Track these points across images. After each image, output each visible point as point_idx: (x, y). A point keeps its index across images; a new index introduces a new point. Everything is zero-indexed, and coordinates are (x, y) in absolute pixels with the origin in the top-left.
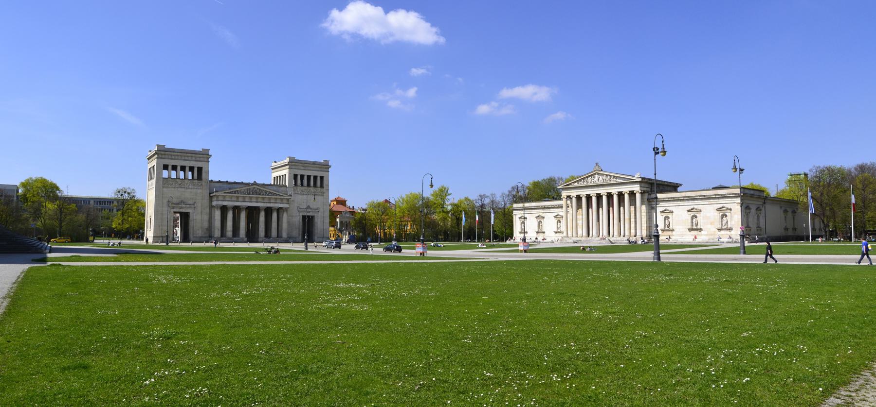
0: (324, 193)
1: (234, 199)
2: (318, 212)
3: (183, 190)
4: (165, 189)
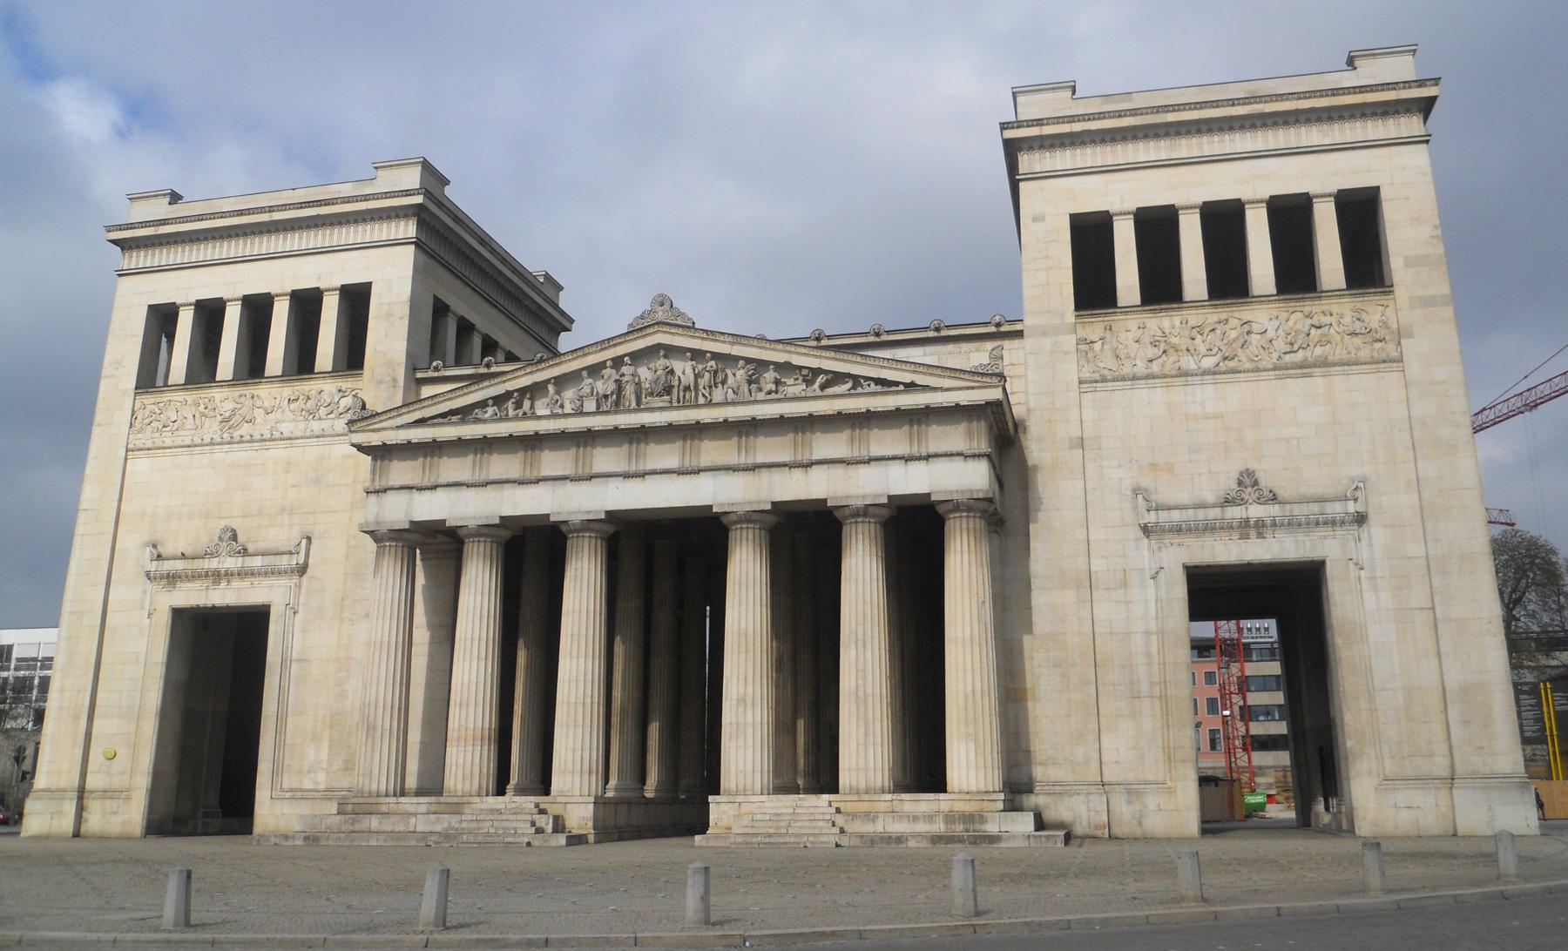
0: (1399, 335)
1: (504, 465)
2: (1361, 519)
3: (240, 454)
4: (138, 465)
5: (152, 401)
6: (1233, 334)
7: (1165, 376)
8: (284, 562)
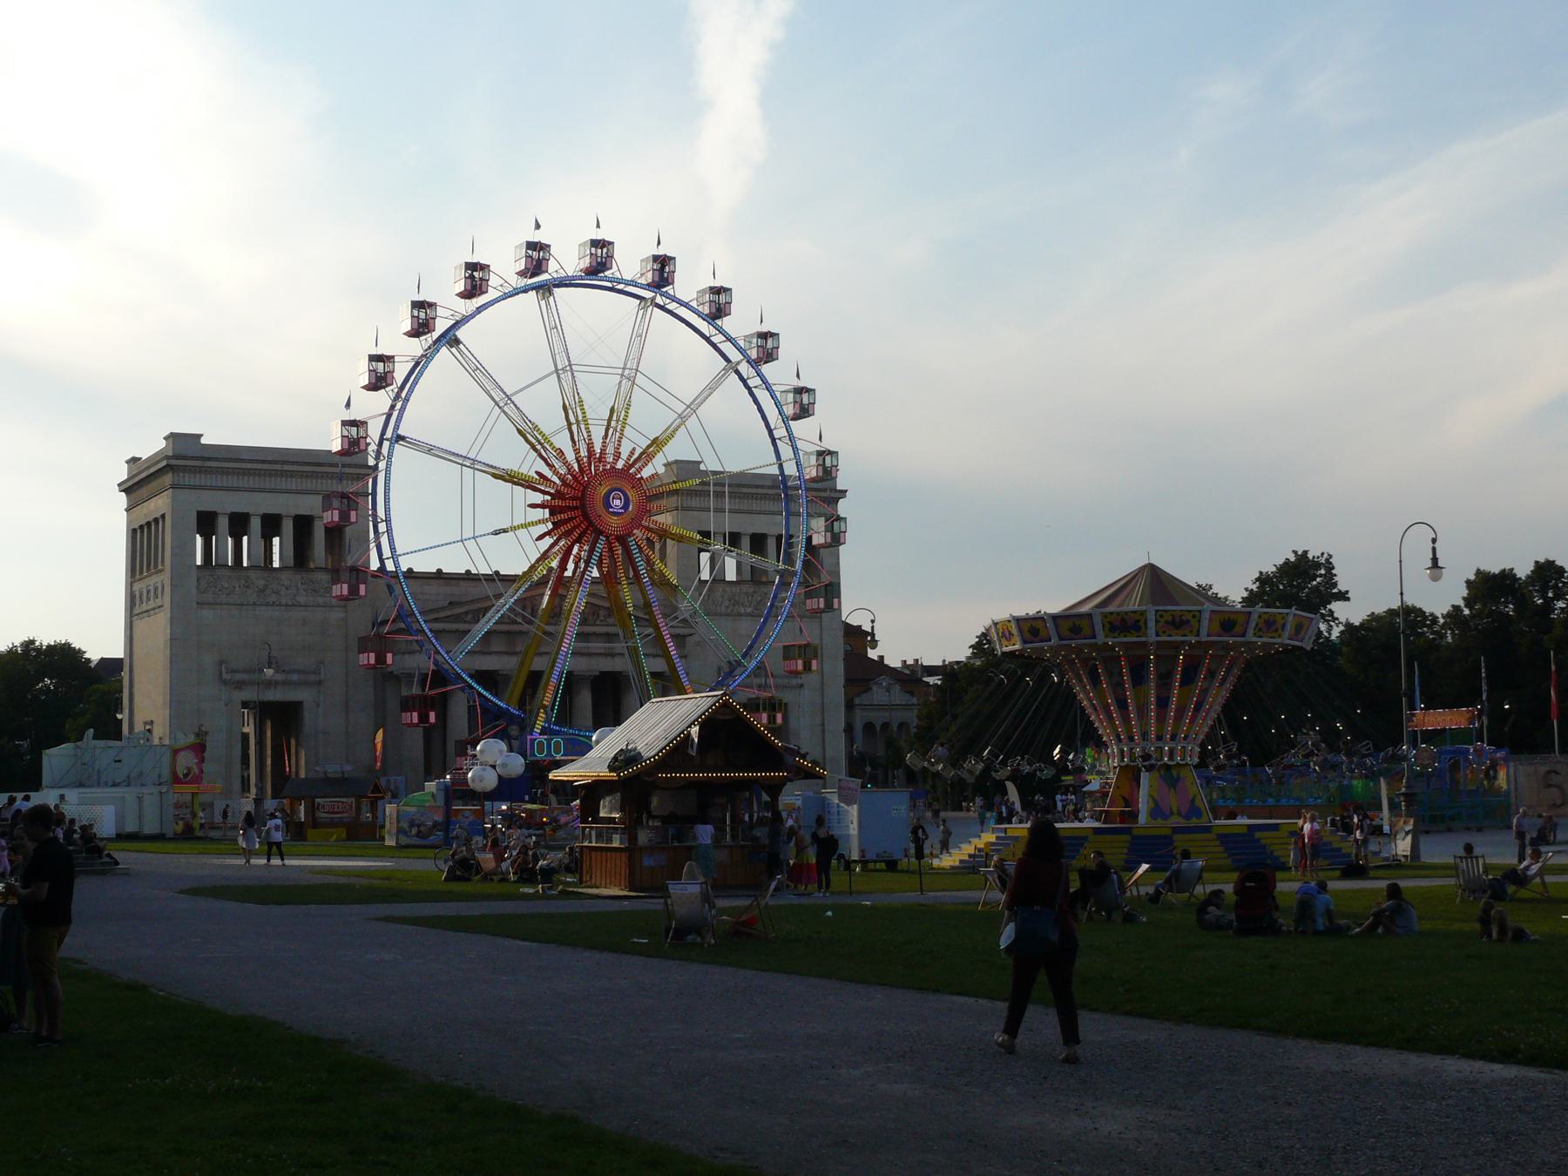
2: (801, 686)
4: (207, 614)
5: (209, 573)
6: (759, 598)
7: (733, 615)
8: (312, 678)
